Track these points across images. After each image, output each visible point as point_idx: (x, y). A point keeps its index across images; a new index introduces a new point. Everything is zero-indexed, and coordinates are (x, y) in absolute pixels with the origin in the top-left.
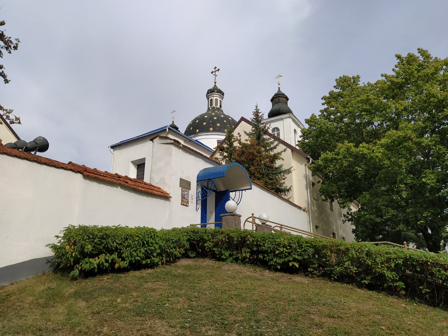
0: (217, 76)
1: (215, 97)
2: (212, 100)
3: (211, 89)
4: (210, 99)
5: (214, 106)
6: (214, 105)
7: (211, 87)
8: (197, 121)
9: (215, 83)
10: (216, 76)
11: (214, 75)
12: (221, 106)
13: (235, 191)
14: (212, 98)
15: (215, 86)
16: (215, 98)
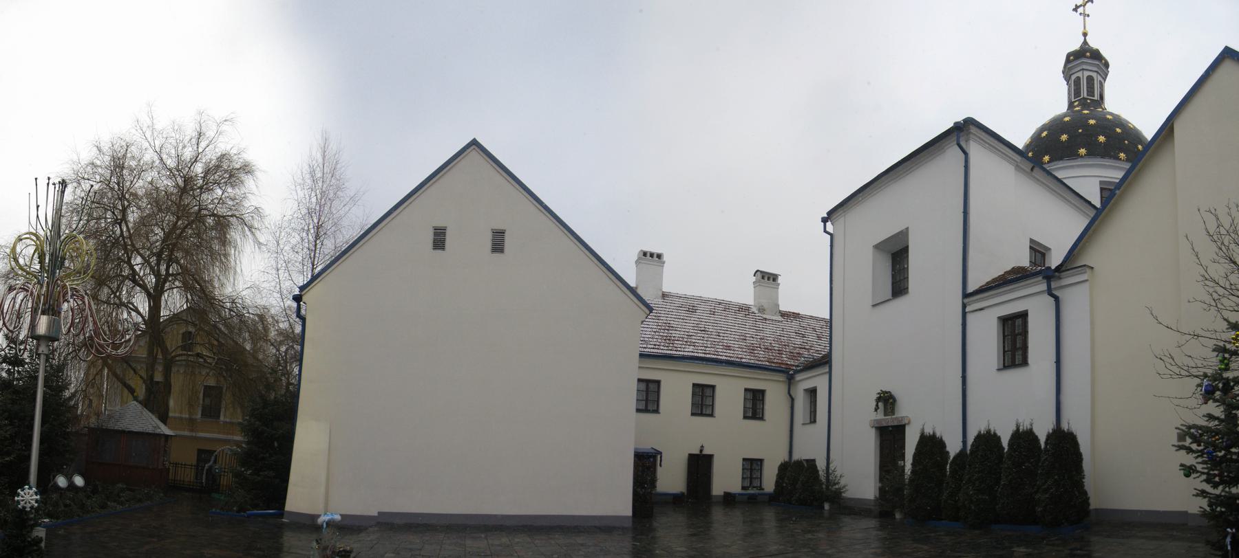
0: (1088, 16)
2: (1078, 80)
4: (1073, 77)
5: (1085, 96)
6: (1084, 93)
7: (1076, 45)
9: (1085, 35)
14: (1079, 74)
15: (1085, 43)
16: (1087, 74)
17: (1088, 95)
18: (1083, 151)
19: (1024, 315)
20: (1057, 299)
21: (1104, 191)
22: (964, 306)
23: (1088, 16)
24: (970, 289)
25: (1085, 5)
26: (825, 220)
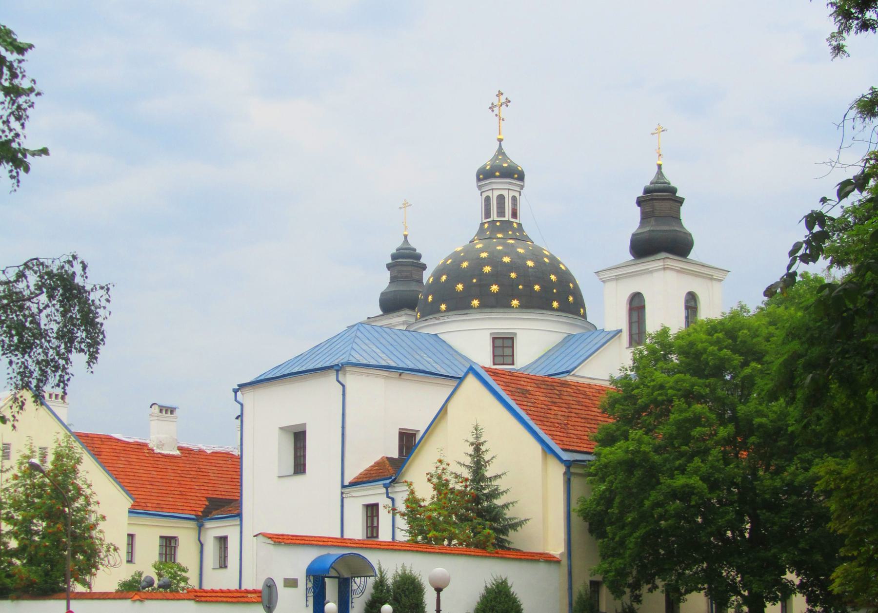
0: (503, 120)
1: (500, 187)
3: (485, 166)
5: (496, 219)
6: (494, 216)
7: (485, 158)
8: (444, 278)
9: (500, 140)
10: (501, 119)
11: (496, 115)
12: (515, 215)
13: (361, 577)
15: (500, 151)
17: (498, 217)
18: (476, 303)
19: (377, 505)
20: (393, 499)
21: (496, 341)
22: (342, 493)
23: (503, 120)
24: (346, 483)
25: (501, 106)
26: (236, 391)
